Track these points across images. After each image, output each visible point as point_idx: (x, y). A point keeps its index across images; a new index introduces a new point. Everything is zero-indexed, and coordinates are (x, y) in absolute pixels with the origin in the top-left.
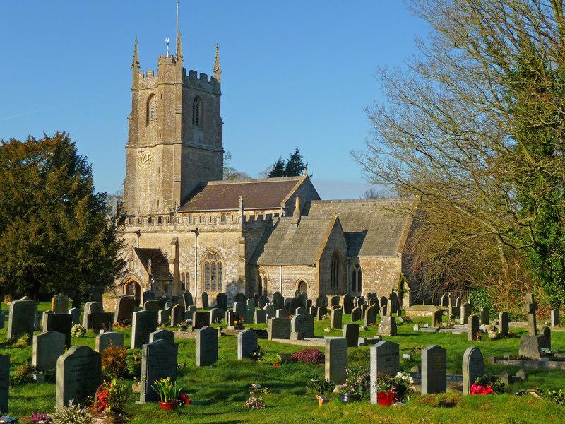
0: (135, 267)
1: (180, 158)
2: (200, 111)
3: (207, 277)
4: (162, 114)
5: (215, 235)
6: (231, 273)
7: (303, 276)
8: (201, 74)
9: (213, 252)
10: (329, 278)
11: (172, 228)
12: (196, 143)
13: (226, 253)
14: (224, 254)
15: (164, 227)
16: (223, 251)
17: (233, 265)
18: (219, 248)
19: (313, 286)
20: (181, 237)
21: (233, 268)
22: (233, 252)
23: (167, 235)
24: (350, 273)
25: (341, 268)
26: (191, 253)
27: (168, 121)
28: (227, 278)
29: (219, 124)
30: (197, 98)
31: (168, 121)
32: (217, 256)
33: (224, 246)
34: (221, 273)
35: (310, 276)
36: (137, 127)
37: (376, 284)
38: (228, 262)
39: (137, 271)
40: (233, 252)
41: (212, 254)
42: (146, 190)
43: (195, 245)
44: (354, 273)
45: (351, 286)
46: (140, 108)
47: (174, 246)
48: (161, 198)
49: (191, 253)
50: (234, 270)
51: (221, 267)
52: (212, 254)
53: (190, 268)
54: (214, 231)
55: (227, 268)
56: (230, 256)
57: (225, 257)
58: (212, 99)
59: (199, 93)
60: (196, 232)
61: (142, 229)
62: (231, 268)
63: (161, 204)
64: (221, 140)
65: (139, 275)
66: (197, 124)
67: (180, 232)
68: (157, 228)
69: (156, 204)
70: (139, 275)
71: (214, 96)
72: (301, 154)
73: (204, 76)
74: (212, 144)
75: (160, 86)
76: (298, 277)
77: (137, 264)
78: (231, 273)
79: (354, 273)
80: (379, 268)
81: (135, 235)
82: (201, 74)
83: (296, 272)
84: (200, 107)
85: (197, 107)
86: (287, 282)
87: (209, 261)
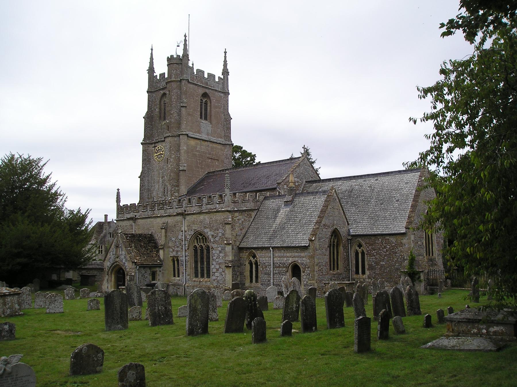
0: (120, 252)
2: (209, 108)
3: (196, 262)
5: (202, 217)
6: (218, 257)
7: (297, 259)
8: (208, 73)
9: (201, 235)
10: (328, 260)
11: (162, 212)
12: (204, 137)
13: (213, 236)
14: (210, 237)
16: (209, 233)
17: (220, 249)
18: (206, 231)
19: (308, 271)
21: (220, 252)
23: (158, 220)
24: (353, 255)
25: (341, 248)
26: (180, 237)
28: (214, 263)
29: (228, 119)
30: (205, 95)
32: (205, 239)
34: (208, 258)
35: (304, 259)
36: (152, 125)
37: (382, 266)
40: (220, 235)
41: (199, 235)
42: (159, 182)
43: (183, 229)
44: (357, 254)
45: (354, 269)
47: (163, 231)
49: (180, 237)
52: (199, 236)
53: (179, 253)
54: (200, 213)
56: (217, 239)
58: (221, 97)
59: (207, 91)
60: (183, 215)
62: (218, 252)
66: (206, 119)
67: (169, 216)
68: (150, 213)
71: (222, 95)
72: (313, 157)
73: (211, 76)
74: (221, 138)
76: (291, 260)
77: (122, 250)
78: (218, 257)
79: (357, 254)
80: (385, 247)
82: (208, 73)
83: (288, 255)
84: (209, 104)
85: (206, 103)
86: (279, 267)
87: (196, 245)
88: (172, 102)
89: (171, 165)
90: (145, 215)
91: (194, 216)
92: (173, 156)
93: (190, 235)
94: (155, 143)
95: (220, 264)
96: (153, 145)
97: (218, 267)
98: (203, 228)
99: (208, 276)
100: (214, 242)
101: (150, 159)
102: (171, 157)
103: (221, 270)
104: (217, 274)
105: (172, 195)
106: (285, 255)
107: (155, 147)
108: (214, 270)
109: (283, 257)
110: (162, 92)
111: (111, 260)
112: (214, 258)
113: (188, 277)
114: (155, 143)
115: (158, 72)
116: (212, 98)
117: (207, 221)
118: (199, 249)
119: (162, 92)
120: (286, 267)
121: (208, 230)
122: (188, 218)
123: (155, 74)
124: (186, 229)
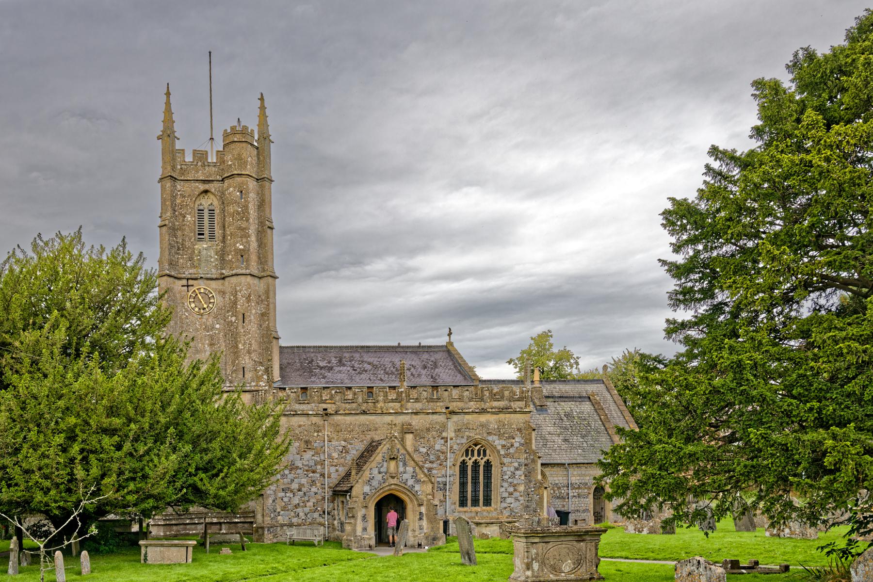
0: (401, 469)
3: (463, 485)
13: (503, 446)
14: (499, 447)
16: (498, 442)
17: (516, 465)
18: (490, 438)
20: (417, 422)
21: (517, 469)
22: (516, 445)
33: (500, 436)
38: (506, 460)
39: (405, 476)
49: (437, 447)
50: (517, 473)
51: (488, 465)
53: (434, 472)
55: (505, 469)
56: (512, 451)
57: (502, 452)
62: (512, 469)
65: (410, 482)
67: (416, 413)
70: (410, 482)
77: (405, 465)
86: (579, 488)
91: (467, 417)
93: (458, 444)
95: (515, 486)
97: (511, 489)
98: (485, 435)
99: (488, 502)
100: (507, 455)
103: (516, 494)
104: (509, 500)
106: (587, 473)
108: (506, 495)
109: (585, 475)
112: (507, 477)
115: (187, 144)
117: (493, 426)
118: (470, 463)
120: (589, 488)
121: (495, 438)
122: (455, 418)
123: (178, 145)
124: (452, 435)
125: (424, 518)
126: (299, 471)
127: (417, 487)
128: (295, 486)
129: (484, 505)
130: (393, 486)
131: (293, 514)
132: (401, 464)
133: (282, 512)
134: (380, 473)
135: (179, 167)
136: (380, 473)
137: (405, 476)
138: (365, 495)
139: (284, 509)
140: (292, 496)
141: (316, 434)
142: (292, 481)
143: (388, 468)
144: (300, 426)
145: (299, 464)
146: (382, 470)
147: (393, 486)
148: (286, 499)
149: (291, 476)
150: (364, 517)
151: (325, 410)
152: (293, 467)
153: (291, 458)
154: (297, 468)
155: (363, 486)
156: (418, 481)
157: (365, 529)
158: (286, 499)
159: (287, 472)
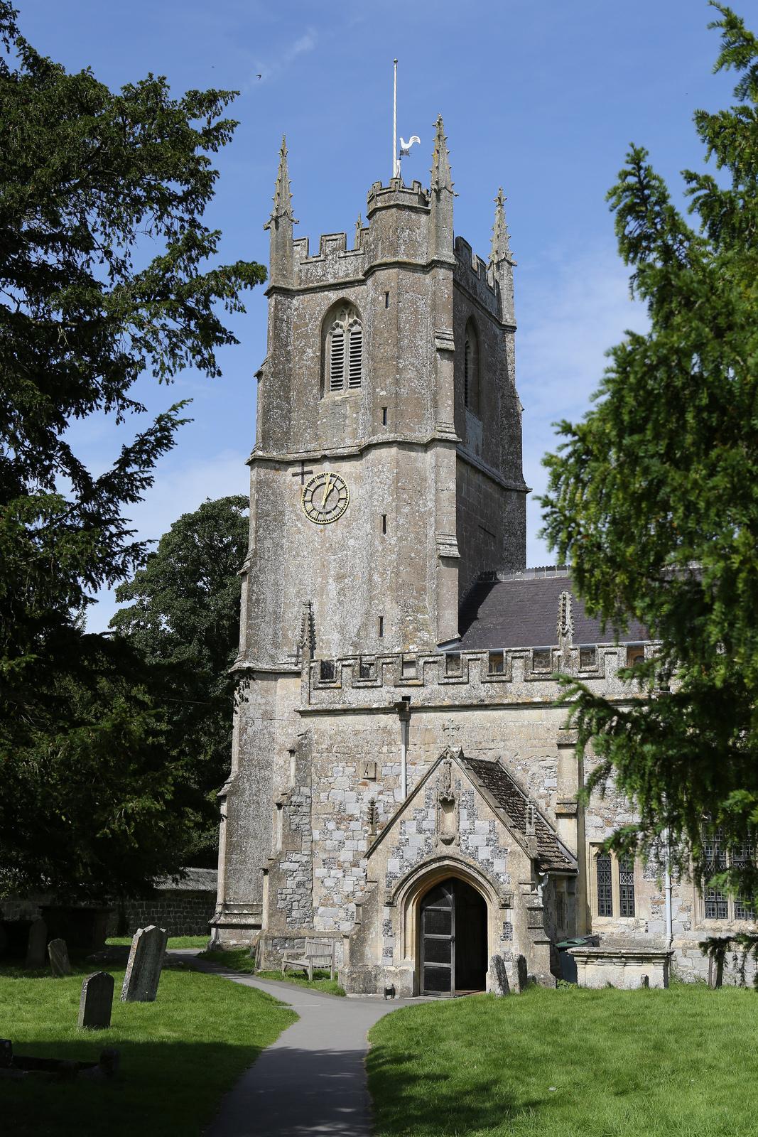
0: (465, 824)
1: (453, 486)
4: (389, 350)
15: (518, 689)
27: (411, 374)
31: (411, 374)
36: (288, 399)
39: (474, 840)
46: (295, 344)
48: (392, 611)
61: (417, 697)
63: (390, 632)
64: (519, 455)
65: (484, 854)
68: (485, 693)
69: (377, 628)
70: (484, 854)
75: (381, 275)
77: (472, 815)
81: (393, 721)
88: (399, 330)
89: (400, 539)
90: (461, 694)
92: (406, 510)
94: (303, 462)
96: (298, 469)
101: (282, 513)
102: (398, 509)
105: (405, 638)
107: (303, 474)
110: (334, 296)
111: (413, 855)
113: (684, 916)
114: (303, 462)
116: (482, 338)
119: (334, 296)
125: (514, 935)
126: (354, 825)
127: (499, 866)
128: (346, 855)
129: (623, 914)
130: (447, 862)
131: (342, 914)
132: (464, 812)
133: (322, 909)
134: (420, 831)
135: (296, 269)
136: (420, 831)
137: (474, 840)
138: (390, 876)
139: (326, 902)
140: (340, 875)
141: (385, 749)
142: (341, 844)
143: (439, 822)
144: (356, 733)
145: (353, 809)
146: (425, 825)
147: (447, 862)
148: (329, 883)
149: (338, 835)
150: (388, 926)
151: (407, 698)
152: (343, 818)
153: (340, 799)
154: (351, 818)
155: (386, 858)
156: (500, 852)
157: (389, 952)
158: (329, 883)
159: (331, 826)
